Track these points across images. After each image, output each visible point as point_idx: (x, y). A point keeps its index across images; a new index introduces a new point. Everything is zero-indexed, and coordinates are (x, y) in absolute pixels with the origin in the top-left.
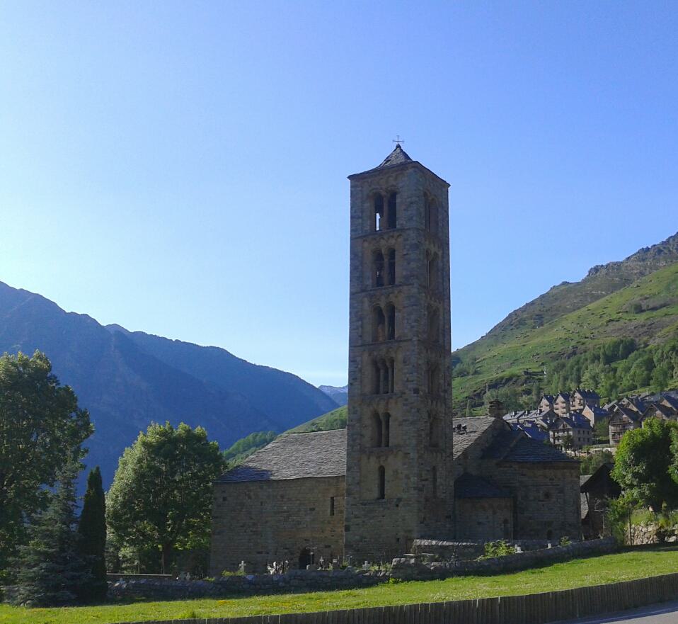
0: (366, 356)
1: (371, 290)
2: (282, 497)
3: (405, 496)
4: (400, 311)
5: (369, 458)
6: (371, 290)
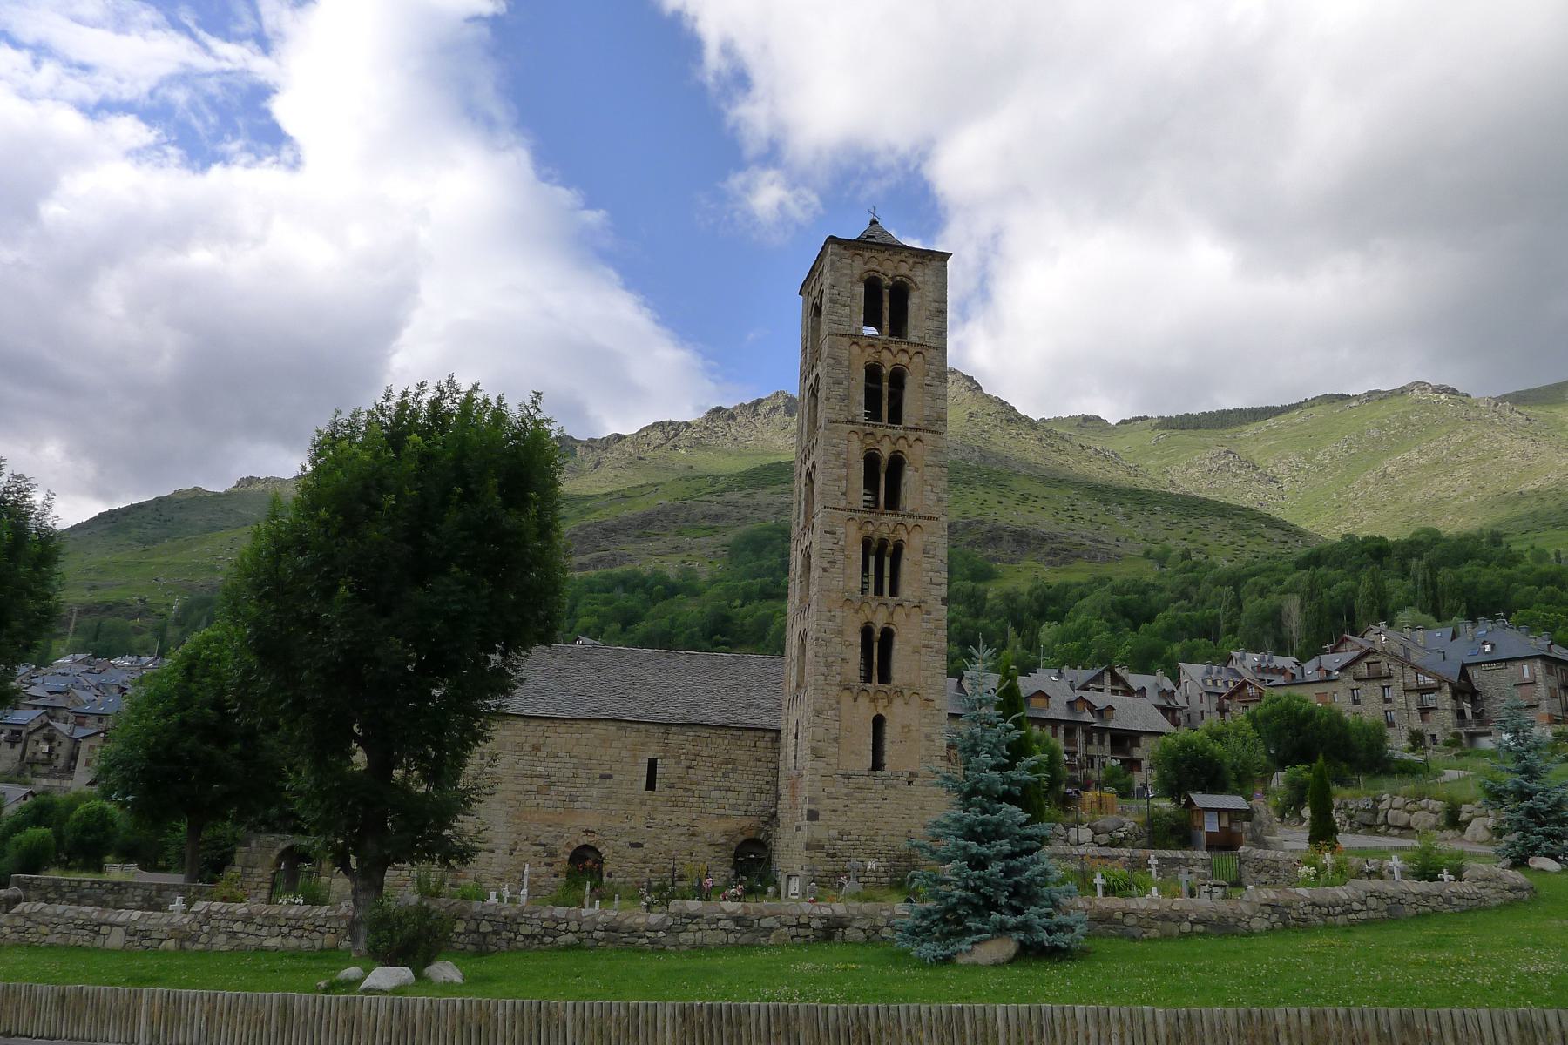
0: (853, 527)
1: (865, 424)
2: (536, 748)
3: (922, 769)
5: (855, 700)
6: (865, 424)
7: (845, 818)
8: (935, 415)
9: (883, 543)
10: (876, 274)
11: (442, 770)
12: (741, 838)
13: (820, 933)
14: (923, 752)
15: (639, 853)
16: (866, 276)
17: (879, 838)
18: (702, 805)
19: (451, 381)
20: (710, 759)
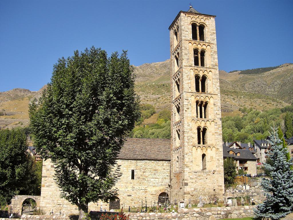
0: (193, 98)
3: (217, 169)
4: (210, 80)
7: (195, 185)
8: (214, 64)
9: (202, 102)
10: (195, 22)
11: (103, 172)
12: (160, 192)
13: (224, 216)
14: (217, 164)
15: (130, 198)
16: (192, 23)
17: (205, 190)
18: (148, 183)
19: (63, 58)
20: (150, 169)
